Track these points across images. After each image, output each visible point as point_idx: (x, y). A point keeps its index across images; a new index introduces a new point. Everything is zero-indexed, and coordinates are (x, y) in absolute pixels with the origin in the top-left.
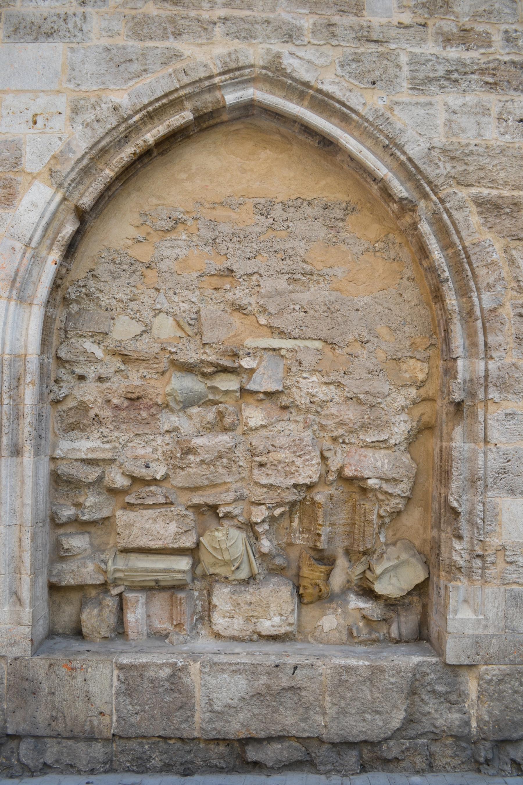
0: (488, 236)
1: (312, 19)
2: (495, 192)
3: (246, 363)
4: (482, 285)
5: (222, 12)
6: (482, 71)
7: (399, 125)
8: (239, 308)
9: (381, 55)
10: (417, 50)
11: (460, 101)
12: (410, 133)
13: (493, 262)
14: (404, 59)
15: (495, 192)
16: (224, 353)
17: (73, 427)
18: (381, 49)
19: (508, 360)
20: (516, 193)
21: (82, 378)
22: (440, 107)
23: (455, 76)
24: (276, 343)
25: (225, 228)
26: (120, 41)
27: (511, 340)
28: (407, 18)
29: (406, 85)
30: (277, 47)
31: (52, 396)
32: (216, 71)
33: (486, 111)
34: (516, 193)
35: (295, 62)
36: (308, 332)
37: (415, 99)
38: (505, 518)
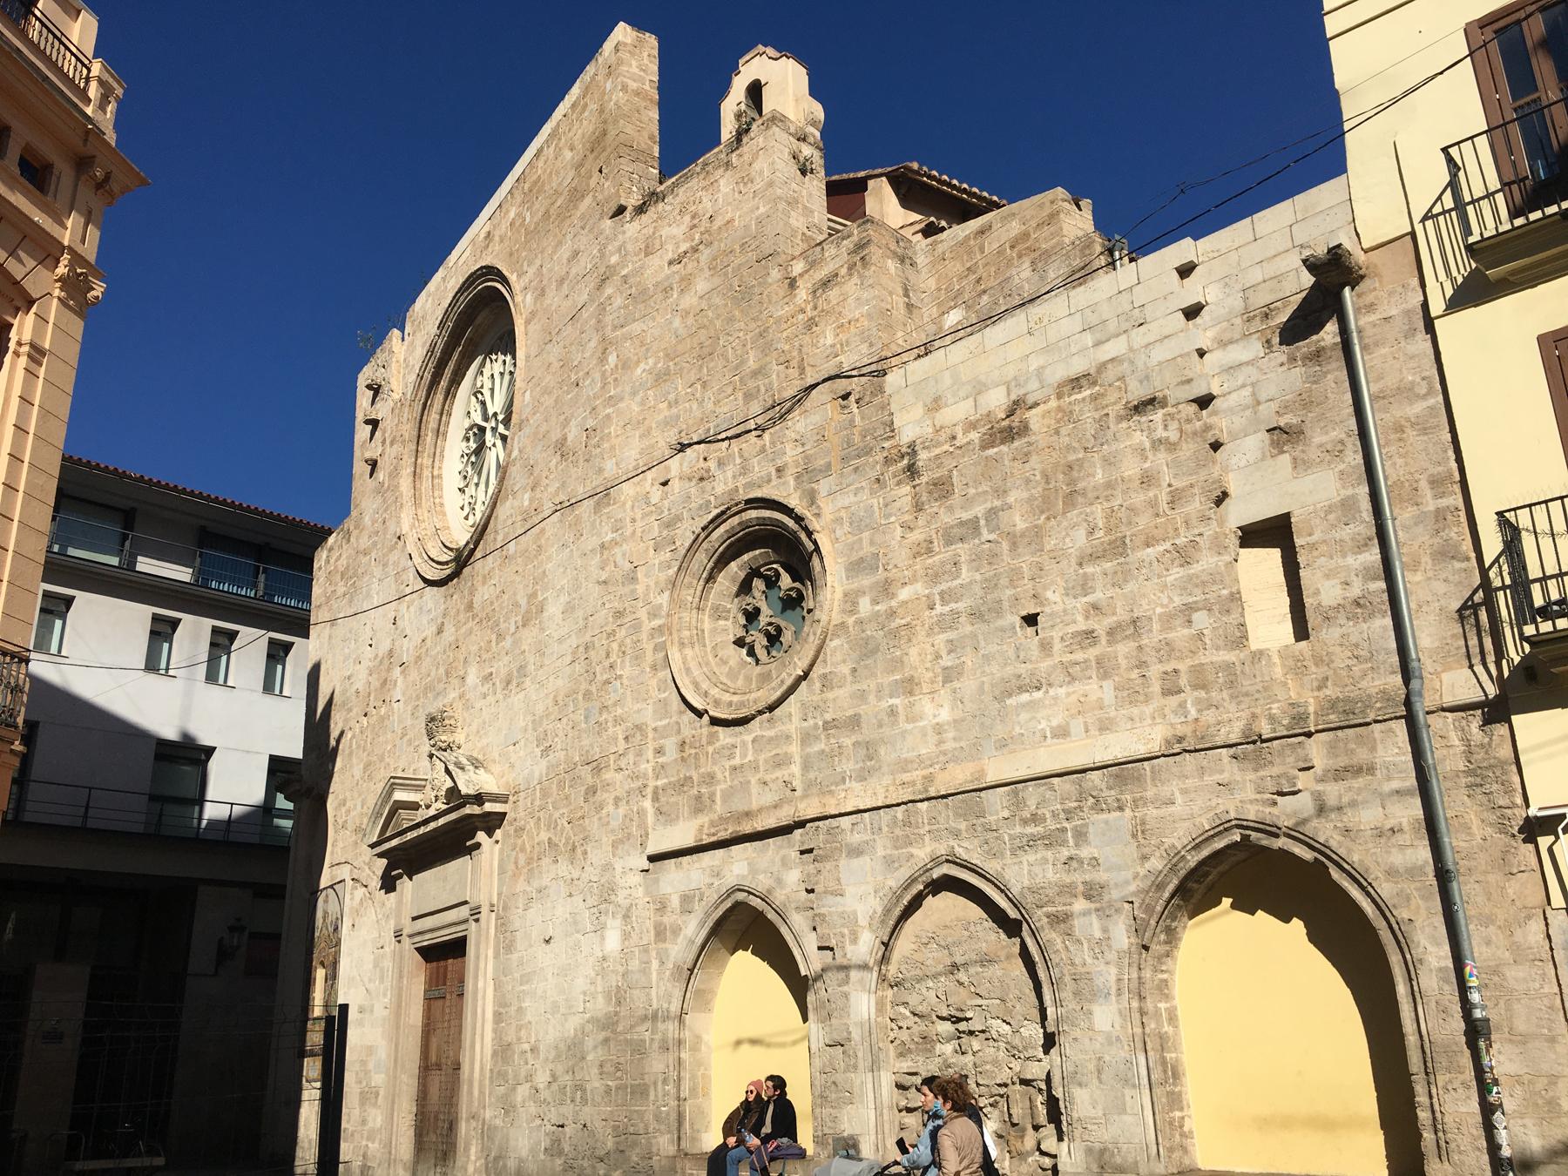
0: (1054, 935)
1: (965, 823)
2: (1054, 909)
3: (969, 1014)
4: (1054, 964)
5: (927, 828)
6: (1043, 838)
7: (1007, 877)
8: (961, 984)
9: (997, 838)
10: (1012, 832)
11: (1034, 858)
12: (1013, 881)
13: (1058, 950)
14: (1007, 838)
15: (1054, 909)
16: (957, 1010)
17: (901, 1055)
18: (995, 834)
19: (1070, 1007)
20: (1064, 908)
21: (900, 1028)
22: (1025, 863)
23: (1031, 843)
24: (979, 1001)
25: (950, 940)
26: (889, 852)
27: (1070, 994)
28: (1006, 814)
29: (1008, 853)
30: (952, 843)
31: (890, 1039)
32: (927, 861)
33: (1045, 860)
34: (1064, 908)
35: (961, 850)
36: (992, 995)
37: (1014, 861)
38: (1078, 1100)
